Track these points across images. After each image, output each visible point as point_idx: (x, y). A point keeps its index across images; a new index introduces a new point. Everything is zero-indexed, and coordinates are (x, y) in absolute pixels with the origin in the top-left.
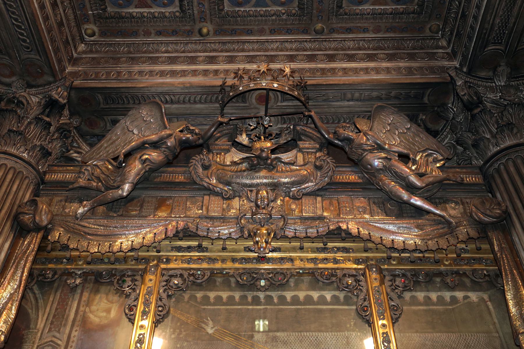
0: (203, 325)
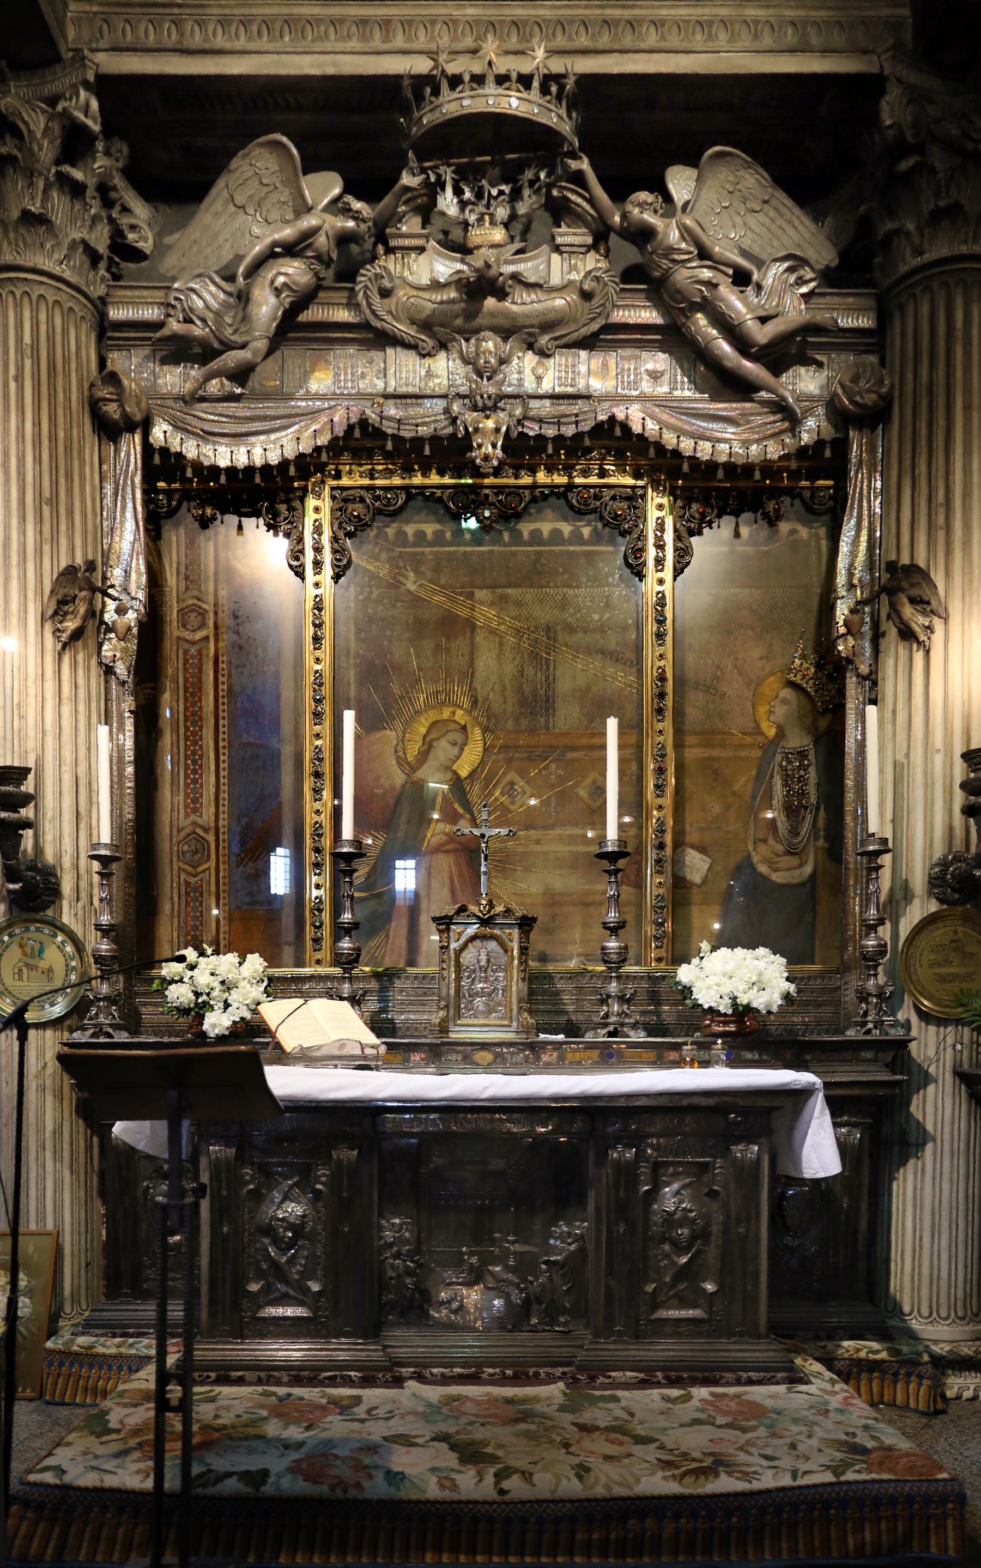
0: (401, 579)
